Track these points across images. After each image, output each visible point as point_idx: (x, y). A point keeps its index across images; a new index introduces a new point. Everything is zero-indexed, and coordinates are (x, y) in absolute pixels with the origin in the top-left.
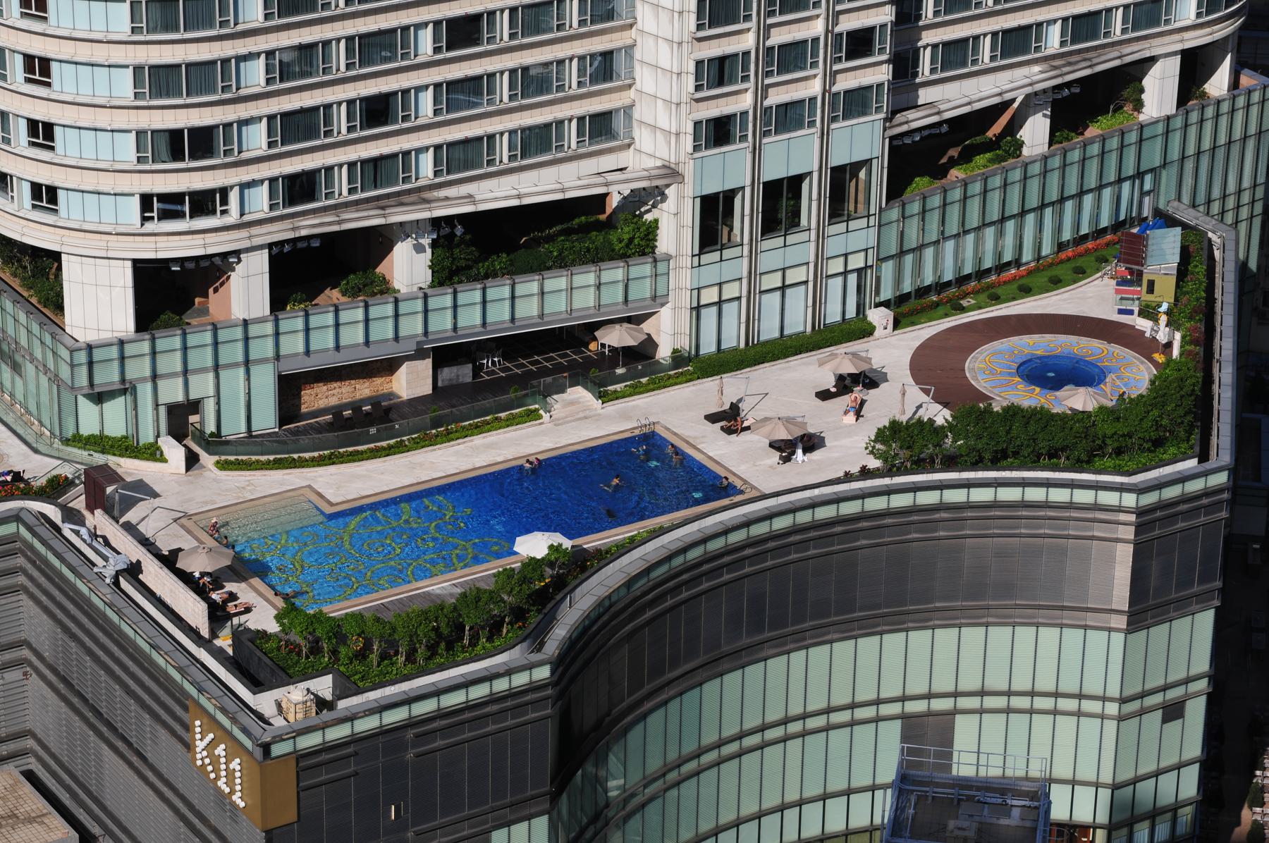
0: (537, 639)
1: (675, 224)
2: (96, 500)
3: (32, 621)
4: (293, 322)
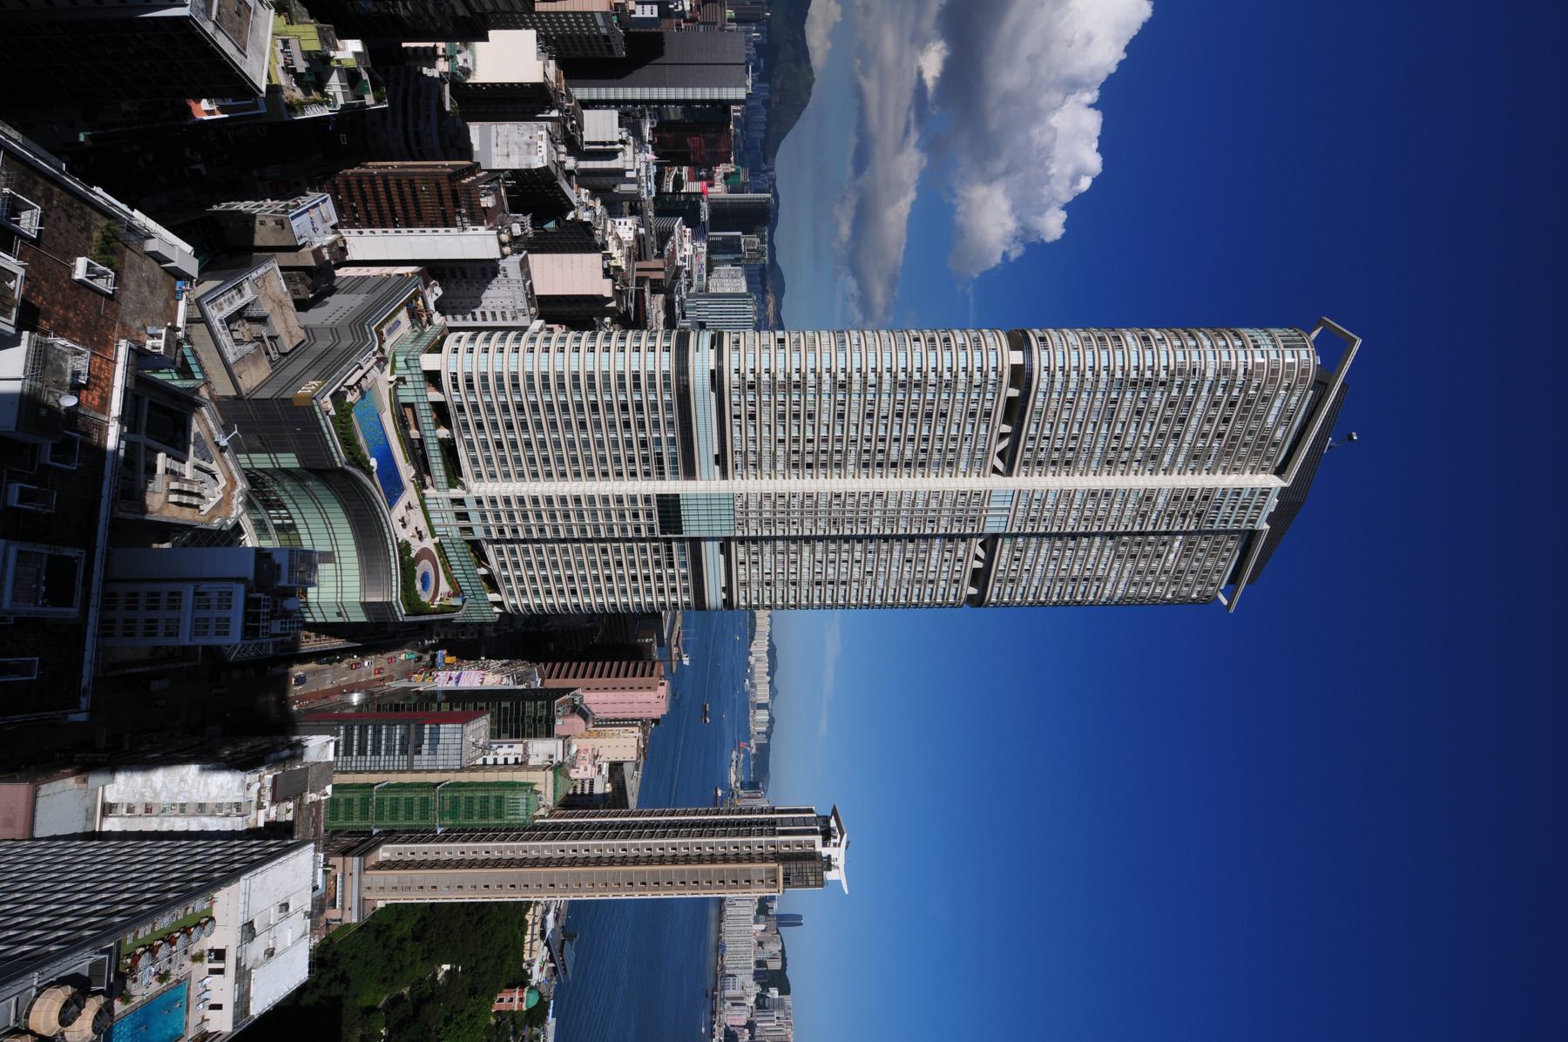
1: (457, 493)
2: (379, 360)
3: (346, 343)
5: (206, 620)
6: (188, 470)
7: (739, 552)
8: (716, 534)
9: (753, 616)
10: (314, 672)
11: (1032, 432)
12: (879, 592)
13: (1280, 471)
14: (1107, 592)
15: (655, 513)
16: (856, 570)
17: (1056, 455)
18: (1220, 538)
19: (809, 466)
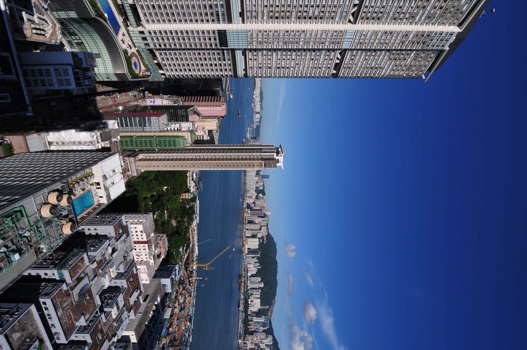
0: (96, 16)
1: (140, 29)
5: (62, 80)
6: (35, 18)
7: (249, 55)
8: (241, 47)
9: (255, 81)
10: (104, 99)
11: (367, 4)
12: (300, 72)
13: (459, 25)
14: (383, 73)
15: (217, 38)
16: (292, 63)
17: (374, 15)
18: (429, 53)
19: (277, 18)
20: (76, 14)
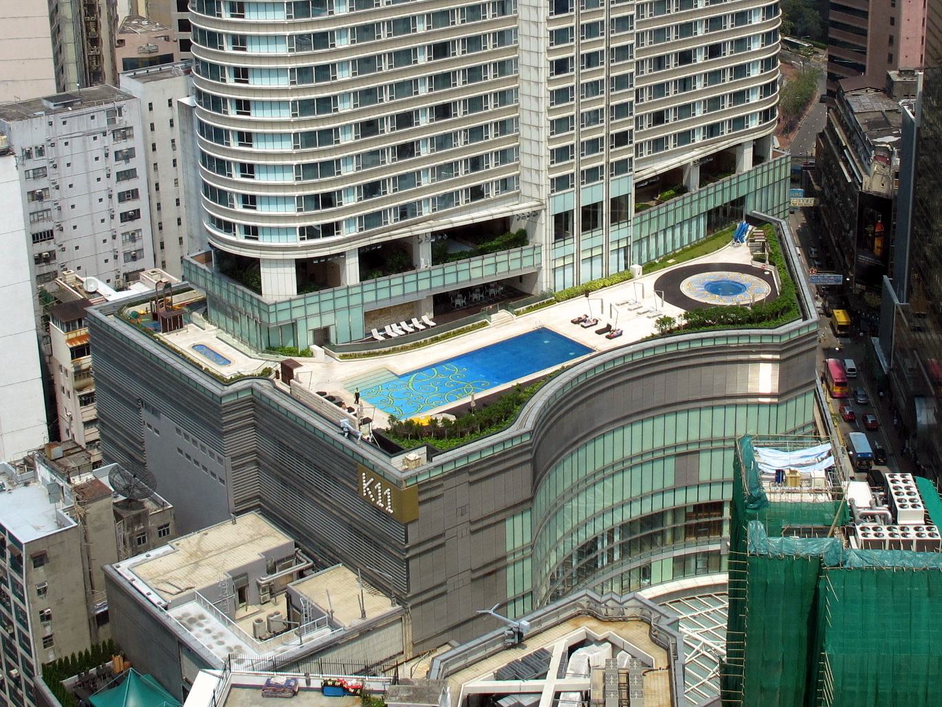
1: (545, 230)
4: (369, 285)
20: (518, 519)
